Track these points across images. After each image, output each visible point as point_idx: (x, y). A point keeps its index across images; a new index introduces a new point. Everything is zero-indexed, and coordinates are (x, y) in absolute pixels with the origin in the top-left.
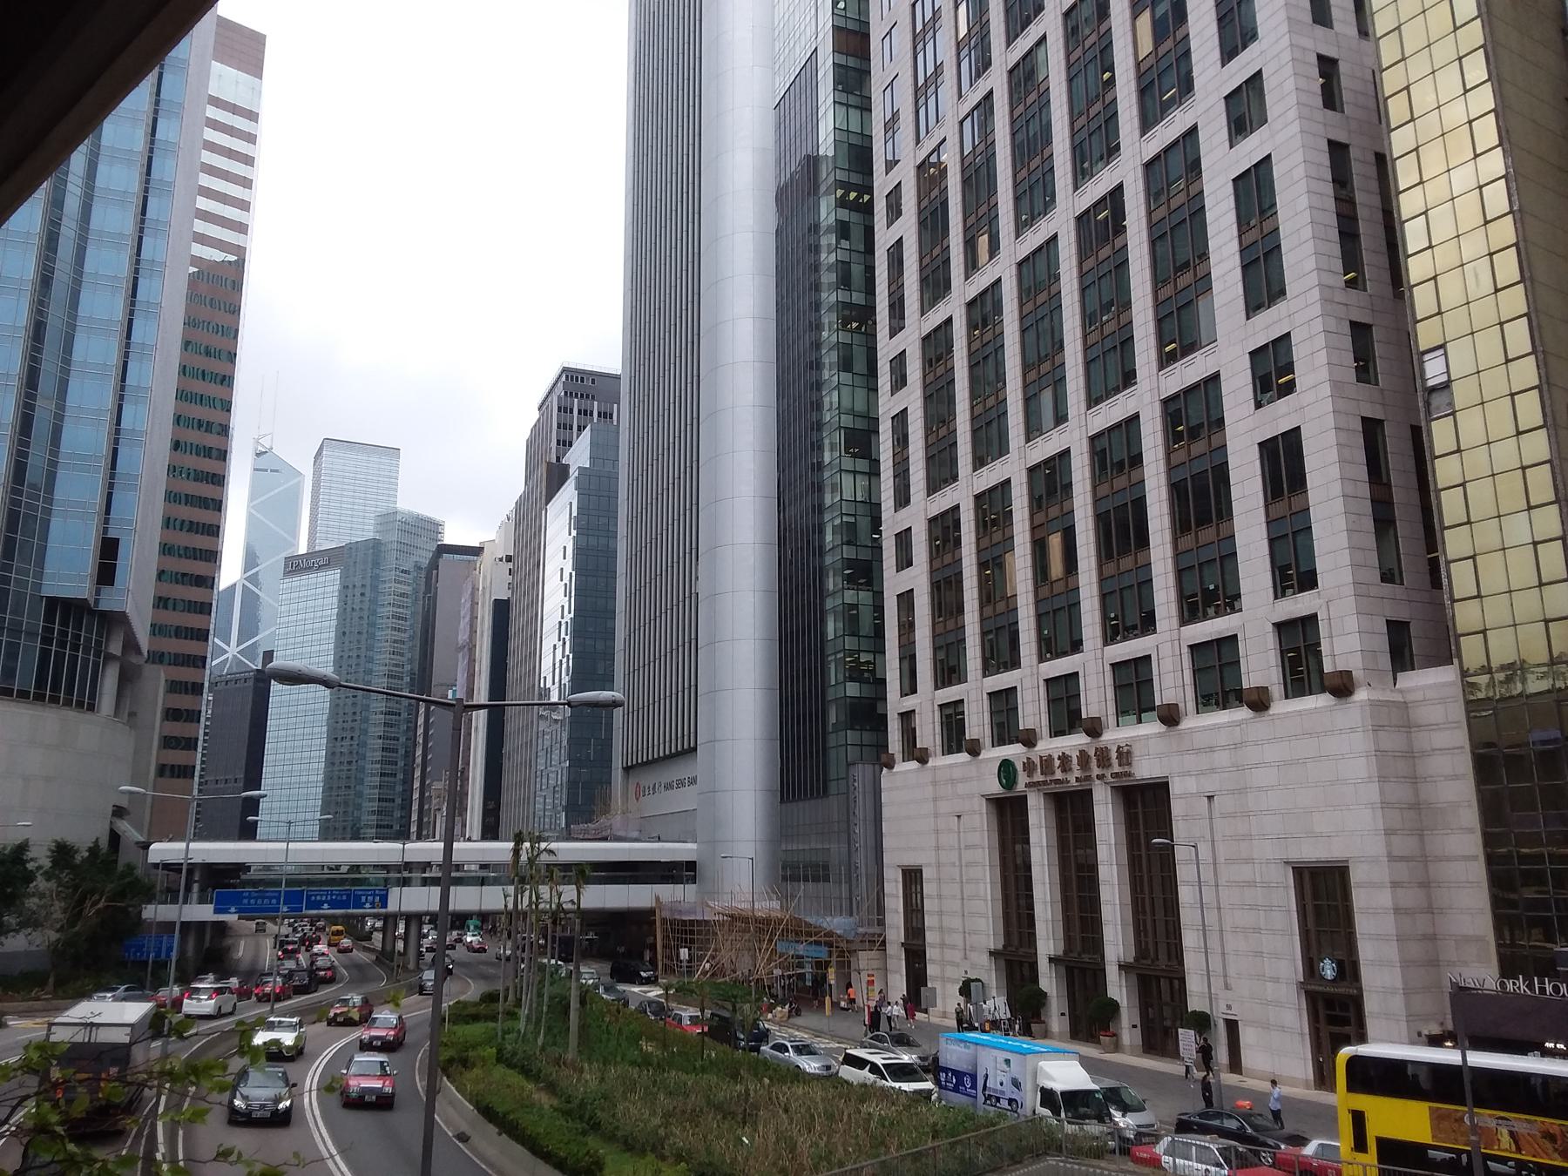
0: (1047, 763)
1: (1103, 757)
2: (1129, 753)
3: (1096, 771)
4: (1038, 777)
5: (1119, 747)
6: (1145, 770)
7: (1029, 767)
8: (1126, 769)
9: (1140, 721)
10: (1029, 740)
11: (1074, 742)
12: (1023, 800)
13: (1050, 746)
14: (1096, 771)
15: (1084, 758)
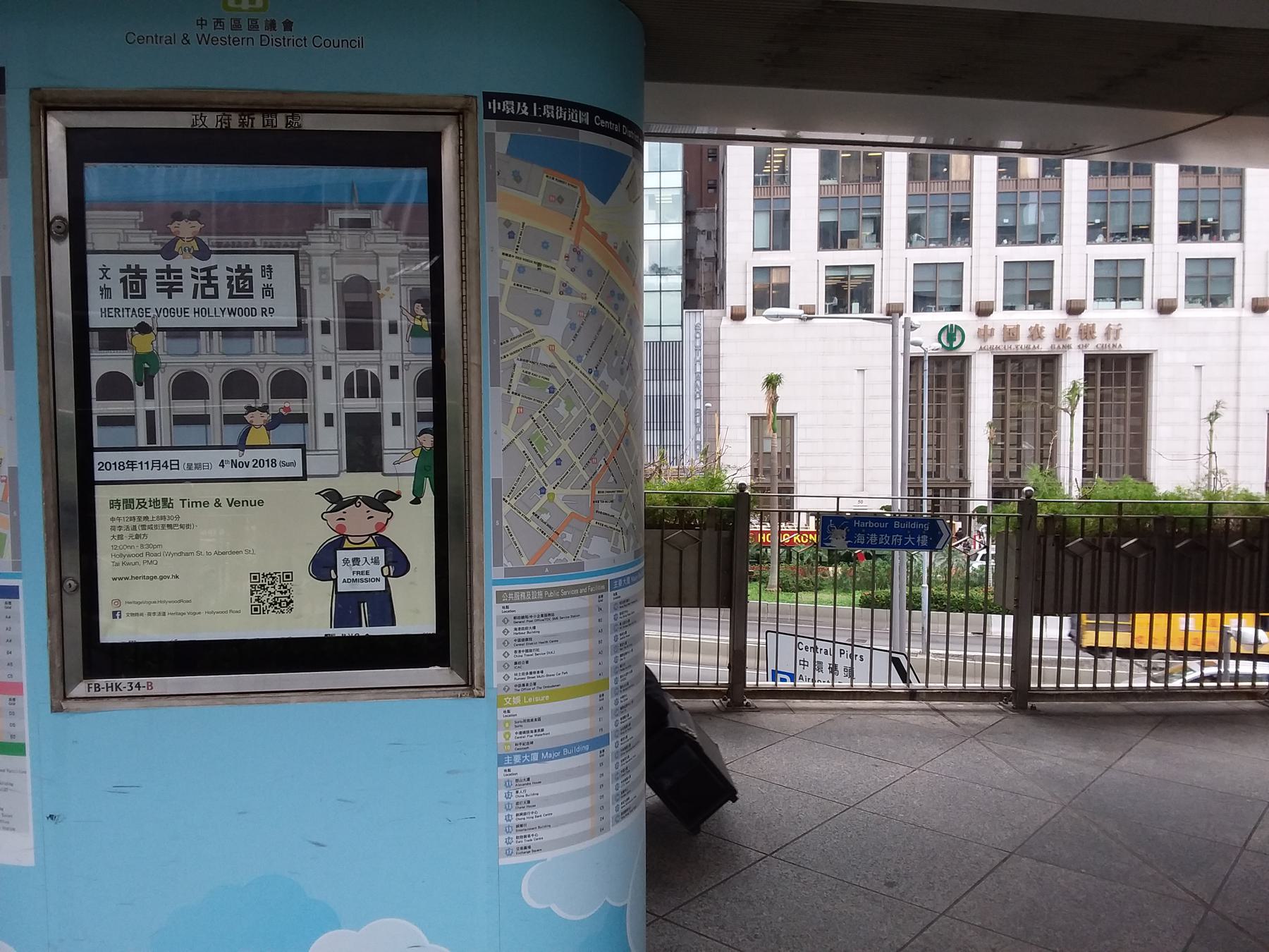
0: (1011, 334)
1: (1087, 333)
2: (1117, 332)
3: (1074, 341)
4: (996, 341)
5: (1110, 325)
6: (1130, 344)
7: (984, 334)
8: (1111, 342)
9: (1117, 307)
10: (983, 311)
11: (1050, 319)
12: (966, 359)
13: (1001, 318)
14: (1074, 341)
15: (1061, 333)
